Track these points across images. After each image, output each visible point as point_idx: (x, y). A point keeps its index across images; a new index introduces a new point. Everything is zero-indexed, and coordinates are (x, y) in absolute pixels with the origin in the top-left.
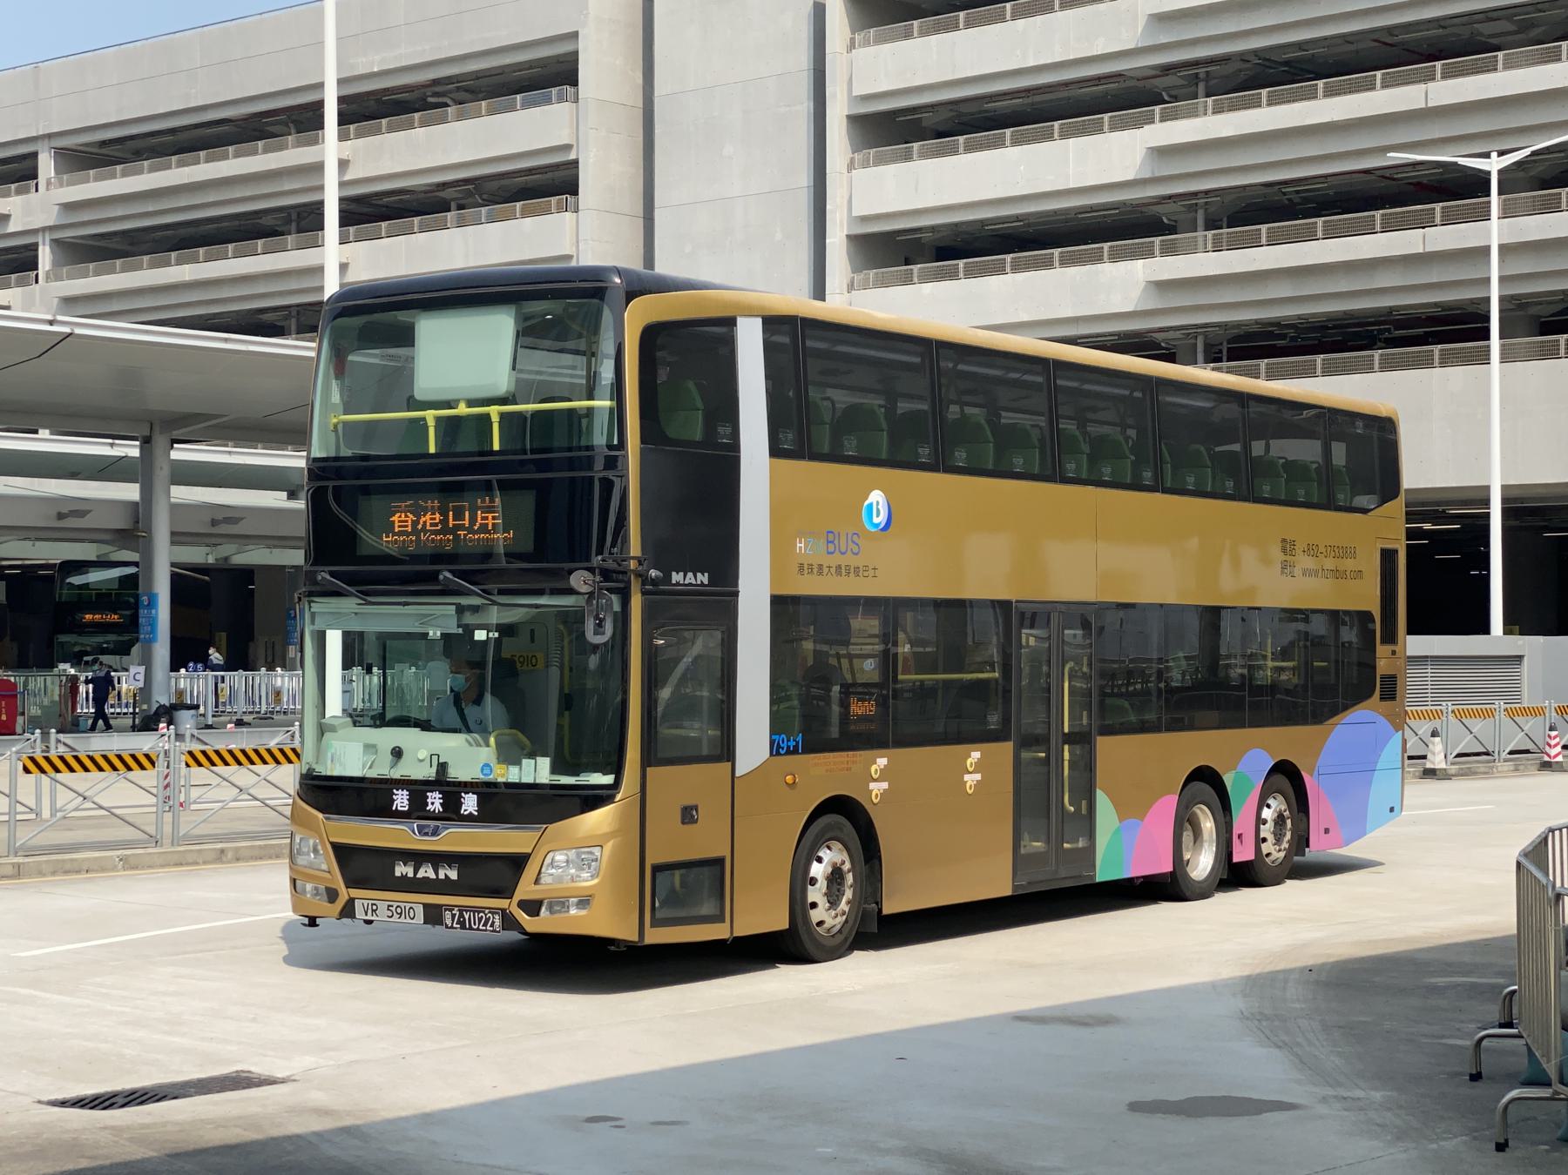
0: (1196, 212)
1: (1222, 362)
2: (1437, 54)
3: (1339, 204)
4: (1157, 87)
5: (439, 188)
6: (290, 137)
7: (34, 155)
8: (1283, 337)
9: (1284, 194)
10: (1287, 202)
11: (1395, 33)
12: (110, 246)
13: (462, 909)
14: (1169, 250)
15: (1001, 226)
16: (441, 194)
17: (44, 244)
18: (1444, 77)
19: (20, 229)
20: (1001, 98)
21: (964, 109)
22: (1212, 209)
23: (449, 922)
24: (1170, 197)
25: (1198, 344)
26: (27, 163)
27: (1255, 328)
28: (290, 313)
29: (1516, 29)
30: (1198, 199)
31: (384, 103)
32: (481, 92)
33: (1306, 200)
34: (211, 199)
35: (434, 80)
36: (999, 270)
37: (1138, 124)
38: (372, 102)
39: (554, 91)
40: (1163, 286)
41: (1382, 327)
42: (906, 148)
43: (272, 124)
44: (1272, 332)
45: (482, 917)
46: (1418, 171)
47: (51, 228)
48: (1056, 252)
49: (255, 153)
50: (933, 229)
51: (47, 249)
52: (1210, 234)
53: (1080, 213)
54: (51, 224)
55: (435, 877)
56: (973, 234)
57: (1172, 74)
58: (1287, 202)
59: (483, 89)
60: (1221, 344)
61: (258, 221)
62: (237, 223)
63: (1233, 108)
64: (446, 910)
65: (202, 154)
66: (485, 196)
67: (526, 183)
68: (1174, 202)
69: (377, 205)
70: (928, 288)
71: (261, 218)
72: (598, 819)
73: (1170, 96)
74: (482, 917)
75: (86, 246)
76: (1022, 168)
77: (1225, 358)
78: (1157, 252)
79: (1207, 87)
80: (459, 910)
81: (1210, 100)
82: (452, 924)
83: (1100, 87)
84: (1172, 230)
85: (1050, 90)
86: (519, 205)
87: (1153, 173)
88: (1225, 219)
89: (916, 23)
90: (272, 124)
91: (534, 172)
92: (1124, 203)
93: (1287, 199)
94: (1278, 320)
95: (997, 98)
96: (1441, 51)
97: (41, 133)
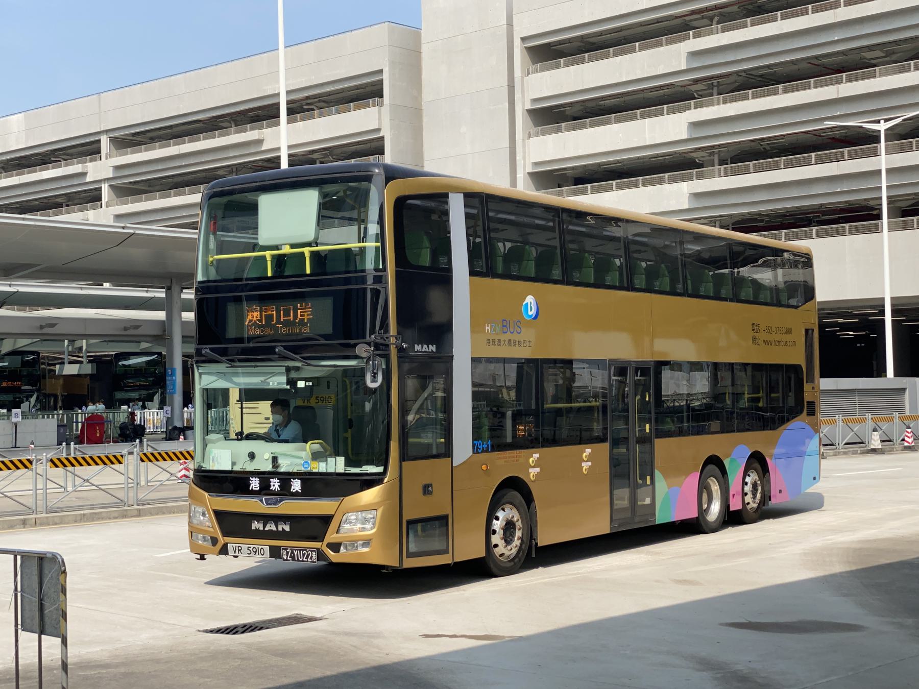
2: (842, 69)
3: (790, 150)
4: (691, 91)
6: (232, 129)
7: (99, 141)
8: (762, 221)
9: (761, 145)
10: (762, 150)
11: (820, 59)
12: (139, 188)
13: (293, 549)
14: (700, 176)
15: (610, 166)
18: (847, 81)
20: (609, 98)
21: (589, 105)
23: (285, 557)
24: (700, 148)
27: (748, 217)
29: (884, 55)
32: (331, 102)
33: (773, 148)
35: (307, 97)
36: (610, 189)
37: (682, 110)
39: (371, 100)
40: (697, 196)
41: (815, 215)
42: (557, 126)
43: (222, 122)
44: (757, 218)
45: (305, 553)
46: (834, 131)
47: (108, 179)
48: (640, 179)
49: (214, 137)
50: (573, 168)
52: (722, 167)
53: (652, 158)
55: (276, 530)
57: (700, 83)
58: (762, 150)
59: (333, 101)
60: (729, 226)
62: (204, 174)
63: (733, 100)
64: (283, 549)
66: (334, 157)
72: (370, 495)
73: (698, 95)
74: (305, 553)
76: (620, 135)
78: (694, 178)
79: (718, 89)
80: (291, 549)
81: (721, 97)
82: (287, 557)
83: (661, 91)
84: (701, 166)
85: (634, 93)
87: (691, 135)
88: (729, 160)
89: (562, 60)
92: (675, 152)
93: (764, 148)
94: (760, 213)
95: (606, 99)
96: (843, 68)
97: (102, 130)
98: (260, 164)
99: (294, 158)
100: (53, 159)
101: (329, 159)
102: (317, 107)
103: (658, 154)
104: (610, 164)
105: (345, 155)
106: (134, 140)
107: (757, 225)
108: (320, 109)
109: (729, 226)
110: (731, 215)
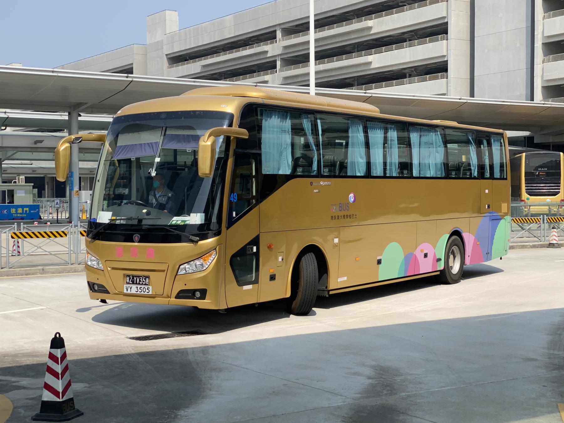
7: (275, 31)
12: (299, 59)
17: (278, 61)
19: (271, 55)
31: (385, 6)
34: (329, 42)
38: (381, 6)
43: (349, 16)
47: (281, 55)
51: (279, 62)
54: (280, 53)
61: (345, 49)
62: (338, 50)
65: (326, 27)
66: (418, 36)
67: (432, 31)
69: (381, 41)
75: (288, 60)
86: (428, 39)
90: (349, 16)
97: (277, 24)
98: (371, 42)
100: (250, 43)
102: (407, 3)
105: (426, 35)
108: (410, 5)
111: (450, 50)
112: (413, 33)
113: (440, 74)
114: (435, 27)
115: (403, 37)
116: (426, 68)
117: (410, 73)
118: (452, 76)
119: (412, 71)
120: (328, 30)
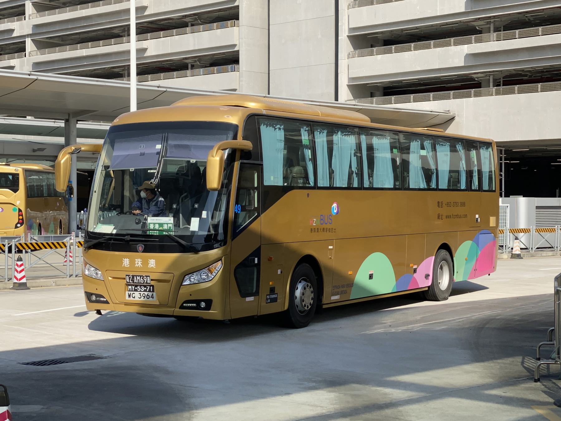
0: (490, 25)
1: (500, 86)
5: (184, 18)
9: (527, 17)
10: (527, 20)
14: (478, 41)
16: (184, 20)
22: (497, 23)
24: (479, 19)
25: (490, 80)
26: (20, 9)
27: (514, 72)
28: (125, 68)
30: (491, 19)
44: (521, 74)
50: (382, 33)
52: (495, 34)
56: (399, 35)
58: (527, 20)
62: (103, 32)
66: (202, 20)
68: (481, 21)
70: (379, 57)
71: (113, 30)
76: (418, 7)
77: (502, 85)
84: (480, 32)
88: (502, 27)
91: (221, 10)
92: (460, 21)
93: (529, 19)
98: (145, 25)
99: (171, 21)
101: (197, 22)
103: (447, 23)
104: (411, 30)
105: (211, 20)
106: (50, 5)
107: (523, 79)
109: (500, 79)
110: (501, 71)
111: (242, 38)
112: (196, 17)
113: (229, 66)
114: (225, 10)
115: (183, 21)
116: (212, 58)
117: (193, 64)
118: (244, 69)
119: (195, 61)
120: (92, 8)
